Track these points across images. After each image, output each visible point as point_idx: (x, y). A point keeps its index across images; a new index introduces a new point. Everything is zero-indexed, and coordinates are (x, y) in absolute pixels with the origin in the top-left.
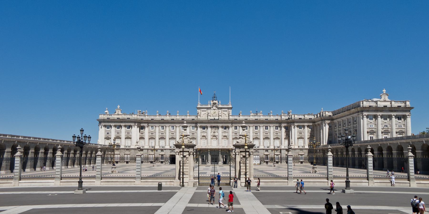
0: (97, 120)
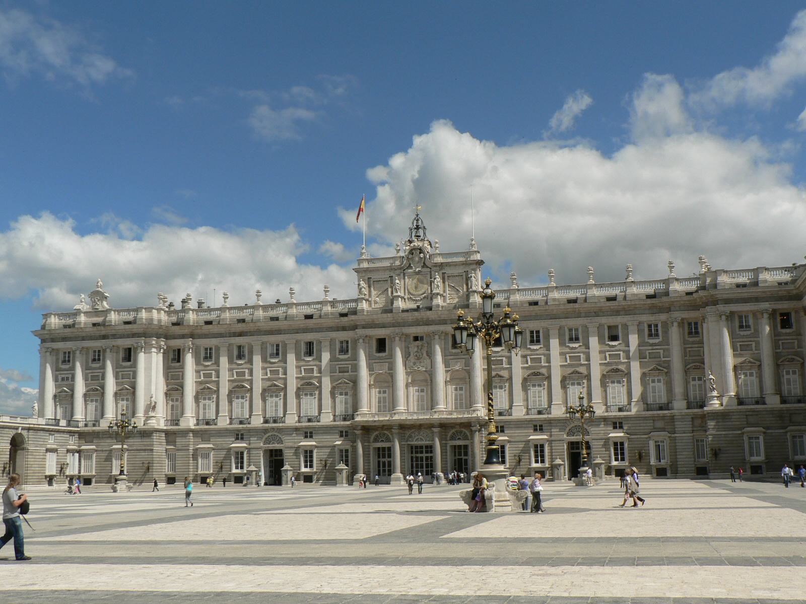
0: (32, 332)
